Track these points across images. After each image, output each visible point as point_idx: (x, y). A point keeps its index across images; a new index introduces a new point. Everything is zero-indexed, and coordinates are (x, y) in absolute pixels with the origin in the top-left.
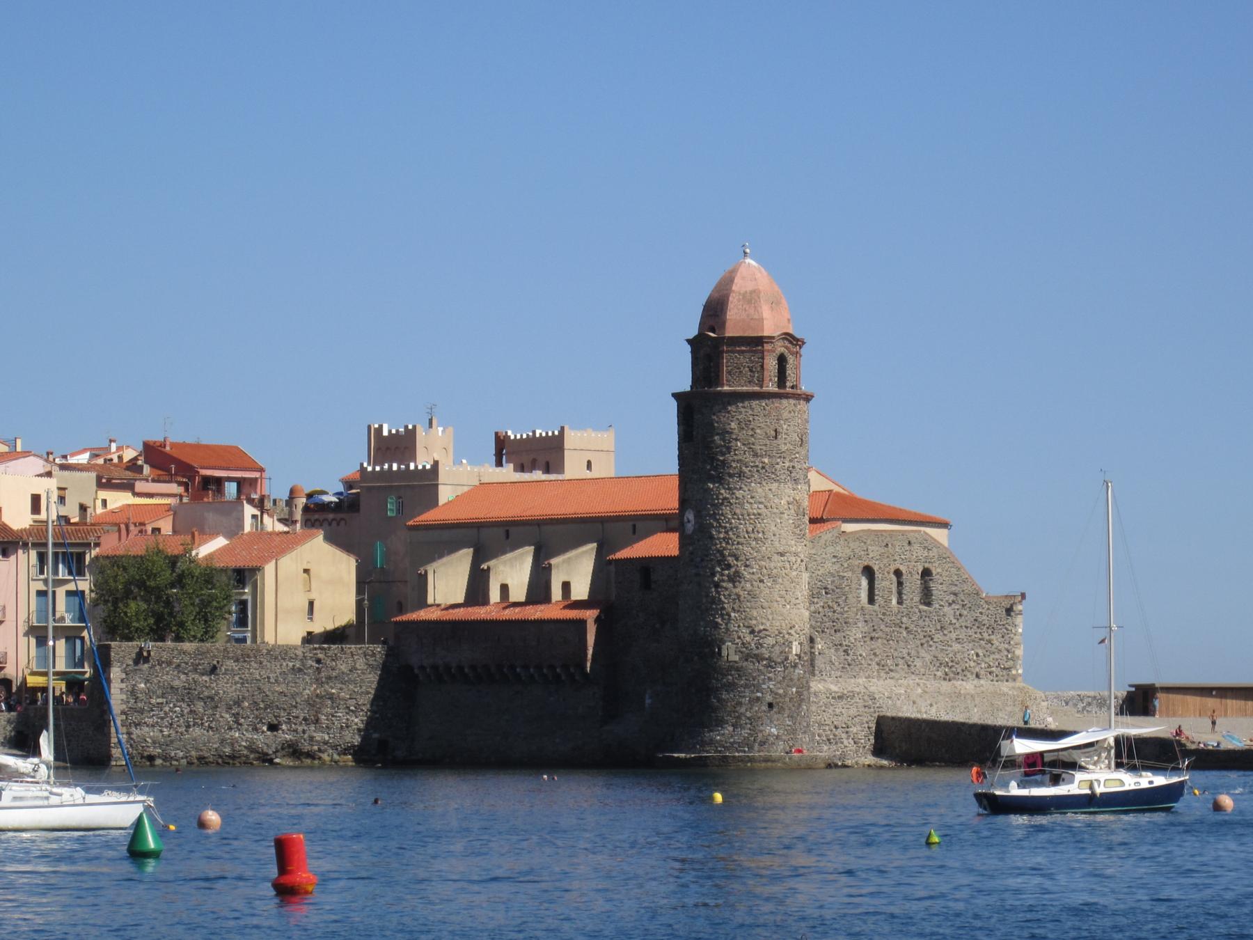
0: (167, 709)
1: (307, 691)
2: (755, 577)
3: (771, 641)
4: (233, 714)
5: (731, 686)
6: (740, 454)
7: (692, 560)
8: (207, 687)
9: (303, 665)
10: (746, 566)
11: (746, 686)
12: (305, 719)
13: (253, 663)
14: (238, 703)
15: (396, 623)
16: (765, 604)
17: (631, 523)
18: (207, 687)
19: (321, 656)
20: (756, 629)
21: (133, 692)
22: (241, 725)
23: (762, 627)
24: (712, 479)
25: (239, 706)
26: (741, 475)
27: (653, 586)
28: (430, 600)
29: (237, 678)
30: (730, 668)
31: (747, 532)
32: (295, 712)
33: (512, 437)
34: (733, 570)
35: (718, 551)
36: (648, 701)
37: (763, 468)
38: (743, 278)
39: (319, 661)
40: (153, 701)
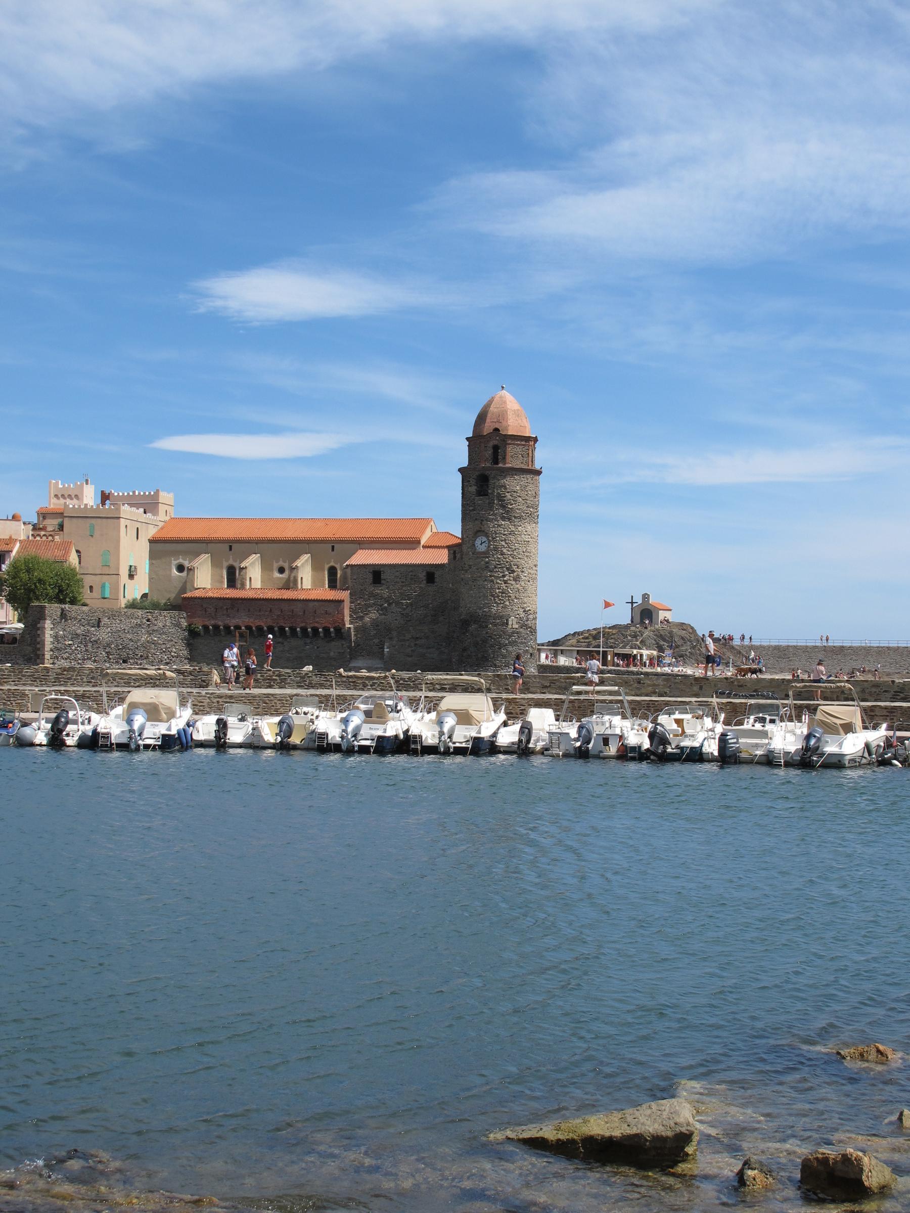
0: (73, 648)
1: (143, 639)
2: (527, 578)
3: (531, 617)
4: (107, 652)
5: (513, 643)
6: (519, 506)
7: (487, 567)
8: (94, 635)
9: (141, 622)
10: (523, 572)
11: (522, 643)
12: (141, 656)
13: (117, 620)
14: (109, 645)
15: (185, 598)
16: (530, 595)
17: (330, 545)
18: (94, 635)
19: (150, 617)
20: (527, 609)
21: (56, 637)
22: (110, 659)
23: (528, 609)
24: (503, 519)
25: (110, 647)
26: (520, 517)
27: (382, 582)
28: (195, 586)
29: (109, 629)
30: (513, 633)
31: (523, 552)
32: (137, 652)
33: (116, 494)
34: (515, 574)
35: (507, 562)
36: (386, 650)
37: (530, 514)
38: (510, 402)
39: (148, 620)
40: (67, 643)
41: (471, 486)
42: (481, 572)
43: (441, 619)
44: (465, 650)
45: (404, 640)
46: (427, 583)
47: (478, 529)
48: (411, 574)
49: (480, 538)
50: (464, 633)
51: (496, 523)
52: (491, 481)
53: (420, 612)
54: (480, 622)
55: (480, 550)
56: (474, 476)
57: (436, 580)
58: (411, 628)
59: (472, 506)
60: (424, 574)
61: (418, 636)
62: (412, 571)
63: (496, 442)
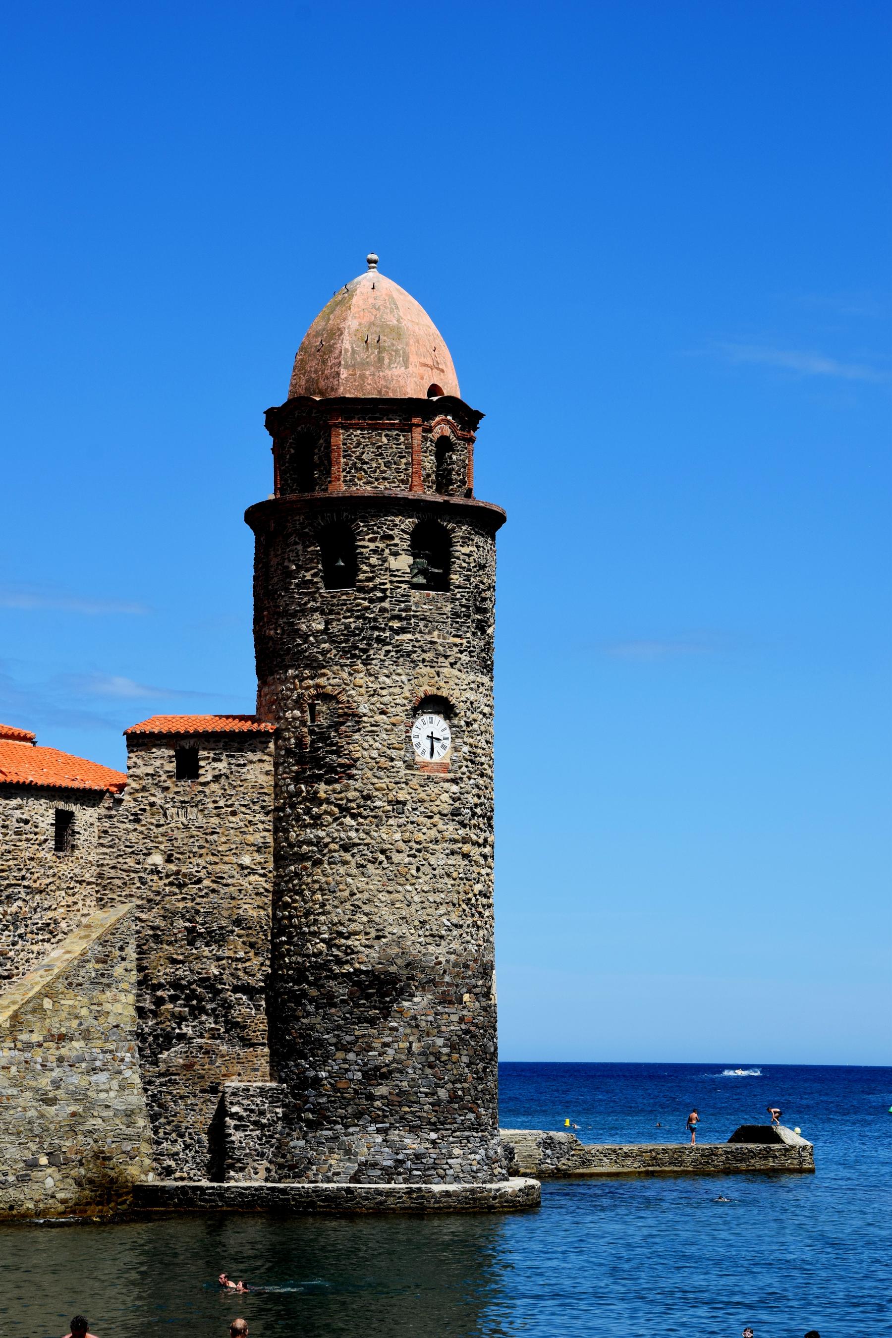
41: (396, 554)
42: (441, 826)
43: (118, 970)
44: (384, 1076)
45: (29, 1046)
46: (55, 850)
47: (432, 691)
48: (18, 814)
49: (426, 717)
50: (372, 1021)
51: (472, 677)
52: (461, 550)
53: (35, 948)
54: (442, 983)
55: (427, 757)
56: (409, 523)
57: (80, 840)
58: (47, 1004)
59: (399, 618)
60: (52, 811)
61: (63, 1030)
62: (20, 807)
63: (447, 431)
